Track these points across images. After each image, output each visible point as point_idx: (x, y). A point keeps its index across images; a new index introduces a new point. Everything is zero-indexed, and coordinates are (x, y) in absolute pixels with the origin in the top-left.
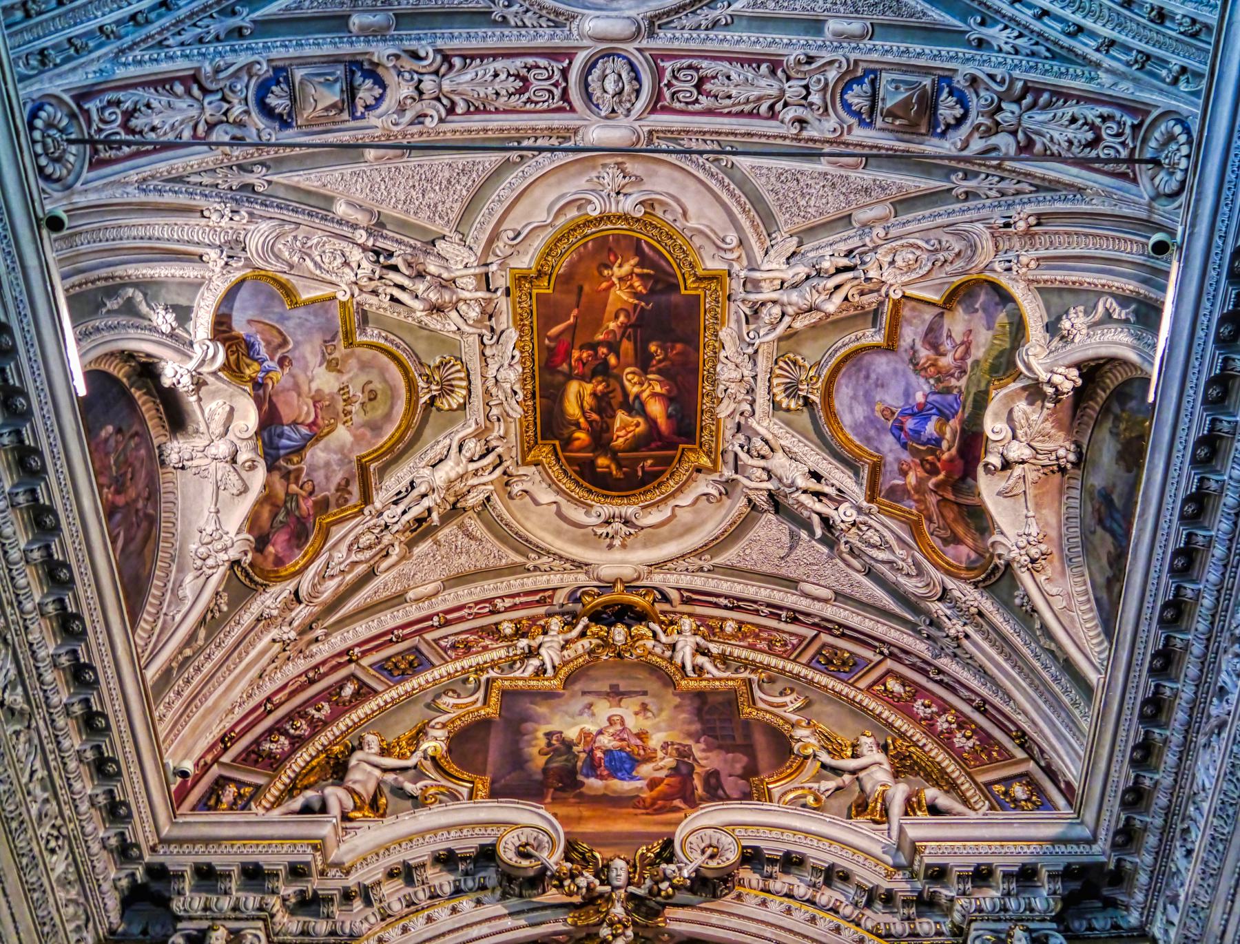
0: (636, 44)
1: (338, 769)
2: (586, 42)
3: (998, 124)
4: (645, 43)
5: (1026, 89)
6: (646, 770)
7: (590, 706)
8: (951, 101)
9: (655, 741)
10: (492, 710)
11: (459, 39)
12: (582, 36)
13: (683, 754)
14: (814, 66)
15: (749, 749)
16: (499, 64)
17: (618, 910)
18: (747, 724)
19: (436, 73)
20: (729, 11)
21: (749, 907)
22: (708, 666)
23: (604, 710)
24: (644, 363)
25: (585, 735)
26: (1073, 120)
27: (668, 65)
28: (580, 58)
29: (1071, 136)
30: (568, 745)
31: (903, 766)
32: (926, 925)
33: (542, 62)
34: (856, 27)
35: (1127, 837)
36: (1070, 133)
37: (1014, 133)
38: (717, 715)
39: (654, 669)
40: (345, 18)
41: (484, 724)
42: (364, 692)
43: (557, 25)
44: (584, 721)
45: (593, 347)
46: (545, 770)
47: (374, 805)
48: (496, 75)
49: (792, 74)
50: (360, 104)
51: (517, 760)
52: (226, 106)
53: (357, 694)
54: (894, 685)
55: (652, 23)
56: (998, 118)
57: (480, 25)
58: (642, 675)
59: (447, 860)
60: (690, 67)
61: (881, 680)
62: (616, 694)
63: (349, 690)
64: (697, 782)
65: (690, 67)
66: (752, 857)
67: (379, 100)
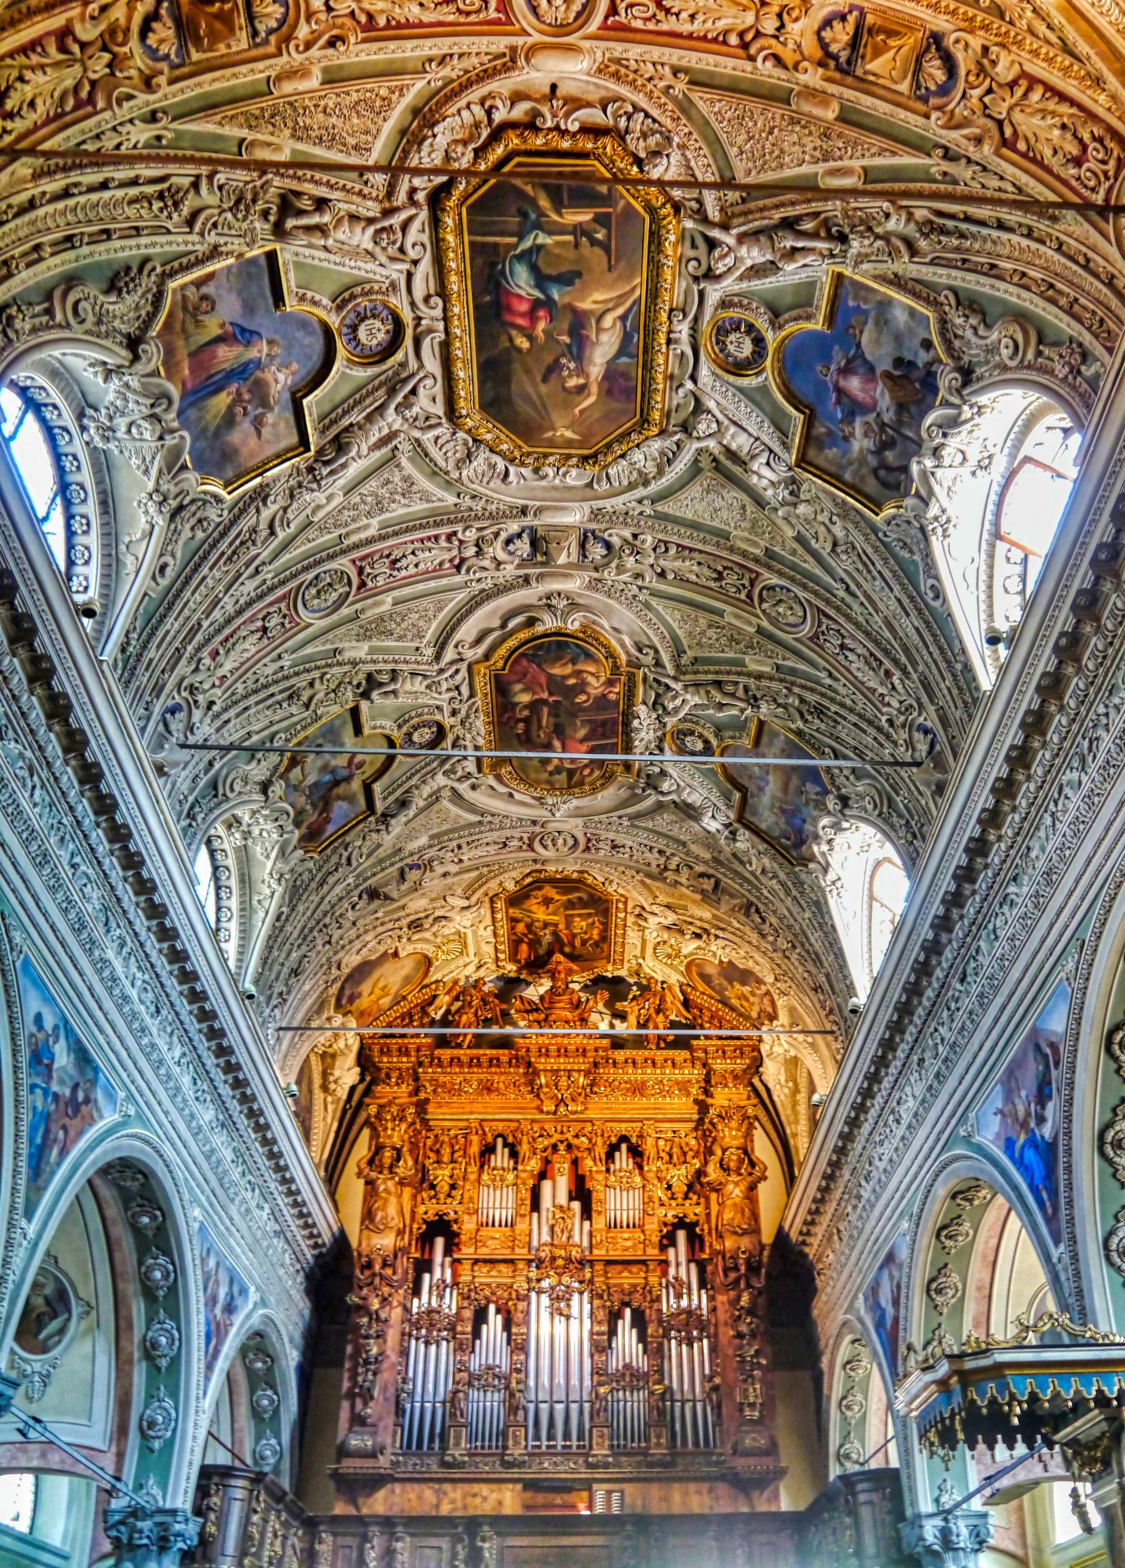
0: (530, 41)
2: (586, 44)
3: (105, 48)
4: (520, 41)
5: (91, 100)
8: (164, 49)
11: (728, 66)
12: (592, 52)
14: (326, 37)
16: (686, 28)
19: (758, 34)
20: (428, 76)
26: (32, 104)
27: (493, 14)
28: (593, 27)
29: (27, 88)
33: (638, 24)
34: (288, 87)
36: (28, 91)
37: (83, 46)
40: (842, 119)
43: (618, 61)
48: (692, 17)
49: (348, 22)
50: (850, 27)
52: (986, 99)
55: (513, 60)
56: (107, 57)
57: (702, 71)
60: (468, 14)
65: (468, 14)
67: (827, 23)
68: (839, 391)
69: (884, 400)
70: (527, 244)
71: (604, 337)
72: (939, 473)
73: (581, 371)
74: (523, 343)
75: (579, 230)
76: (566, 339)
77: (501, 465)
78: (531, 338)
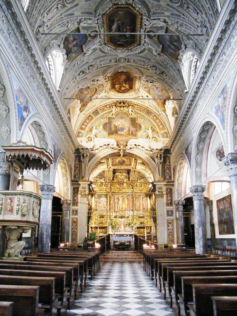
1: (91, 130)
6: (125, 130)
7: (118, 120)
9: (126, 126)
10: (107, 121)
13: (129, 128)
15: (136, 127)
17: (122, 151)
18: (137, 123)
21: (134, 150)
22: (133, 114)
23: (120, 121)
24: (126, 83)
25: (118, 125)
30: (116, 126)
31: (153, 130)
32: (151, 152)
35: (171, 148)
38: (133, 121)
39: (126, 113)
41: (106, 123)
42: (92, 118)
44: (118, 123)
45: (119, 82)
46: (114, 130)
47: (96, 136)
51: (110, 129)
53: (91, 118)
54: (155, 118)
58: (125, 114)
59: (105, 145)
61: (153, 117)
62: (122, 118)
63: (90, 118)
64: (130, 132)
66: (136, 145)
68: (77, 40)
69: (70, 46)
70: (127, 40)
71: (114, 28)
72: (62, 54)
73: (118, 24)
74: (128, 27)
75: (119, 41)
76: (121, 28)
77: (134, 5)
78: (127, 28)
